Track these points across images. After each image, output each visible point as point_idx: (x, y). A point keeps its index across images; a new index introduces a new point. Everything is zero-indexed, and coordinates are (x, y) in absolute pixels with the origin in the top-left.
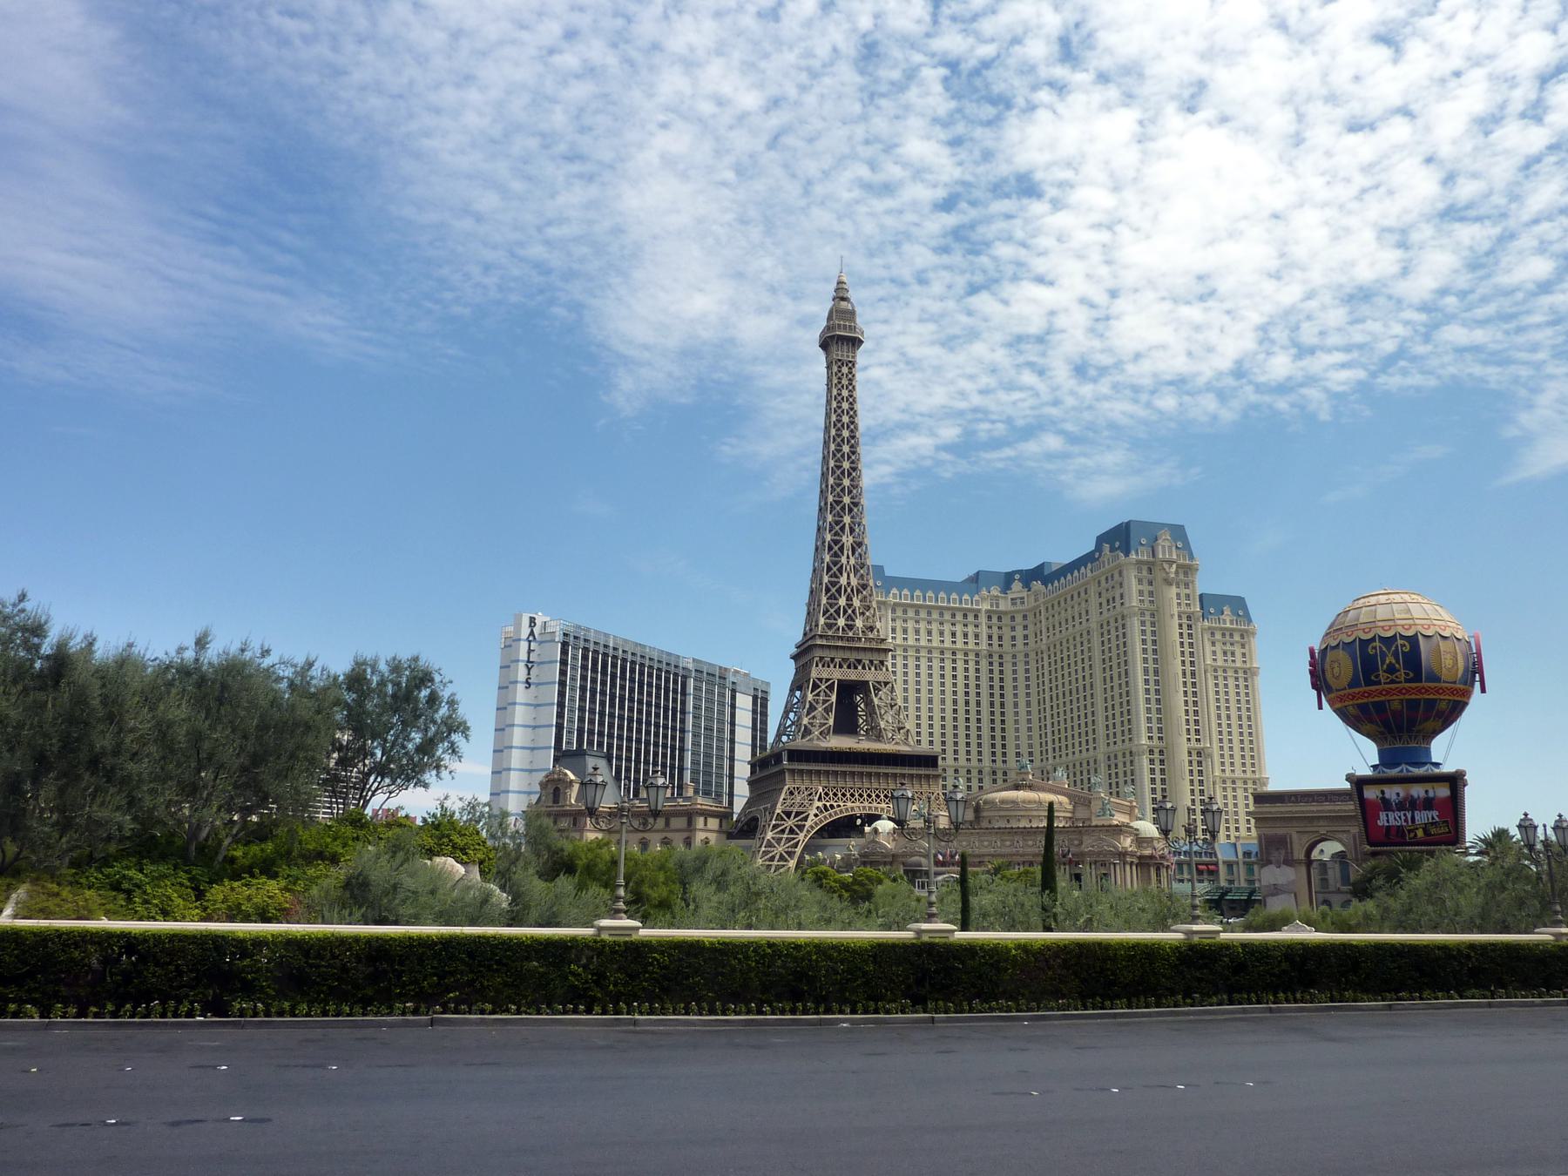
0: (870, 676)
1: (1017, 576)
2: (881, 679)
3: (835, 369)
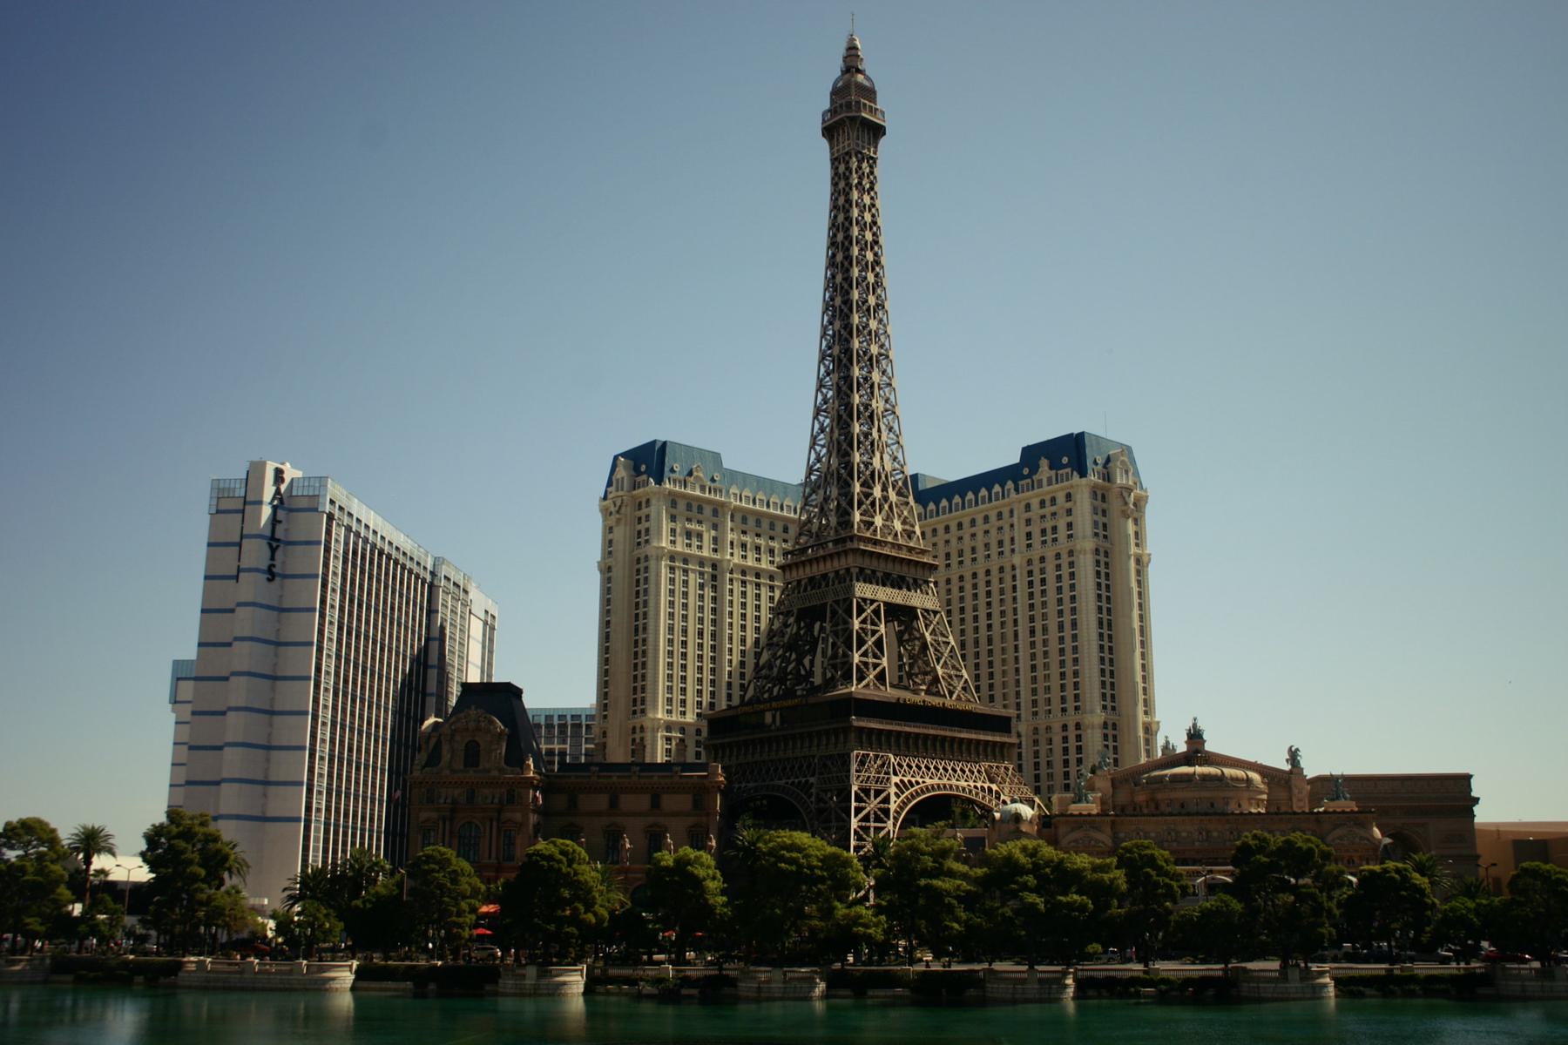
0: (916, 599)
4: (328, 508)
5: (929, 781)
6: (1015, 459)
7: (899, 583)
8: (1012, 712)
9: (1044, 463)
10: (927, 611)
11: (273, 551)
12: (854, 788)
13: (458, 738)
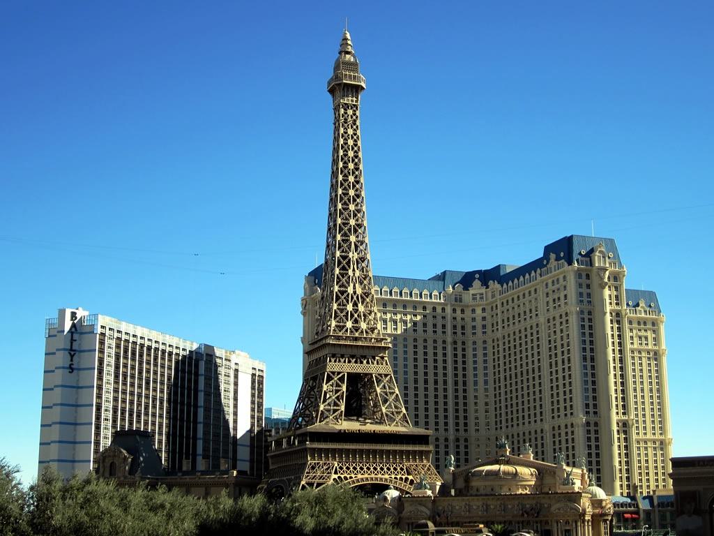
0: (373, 368)
1: (477, 276)
2: (382, 372)
3: (342, 111)
4: (99, 330)
5: (360, 476)
6: (541, 255)
7: (359, 359)
8: (430, 432)
9: (553, 256)
10: (380, 375)
11: (72, 356)
12: (303, 483)
13: (107, 460)
